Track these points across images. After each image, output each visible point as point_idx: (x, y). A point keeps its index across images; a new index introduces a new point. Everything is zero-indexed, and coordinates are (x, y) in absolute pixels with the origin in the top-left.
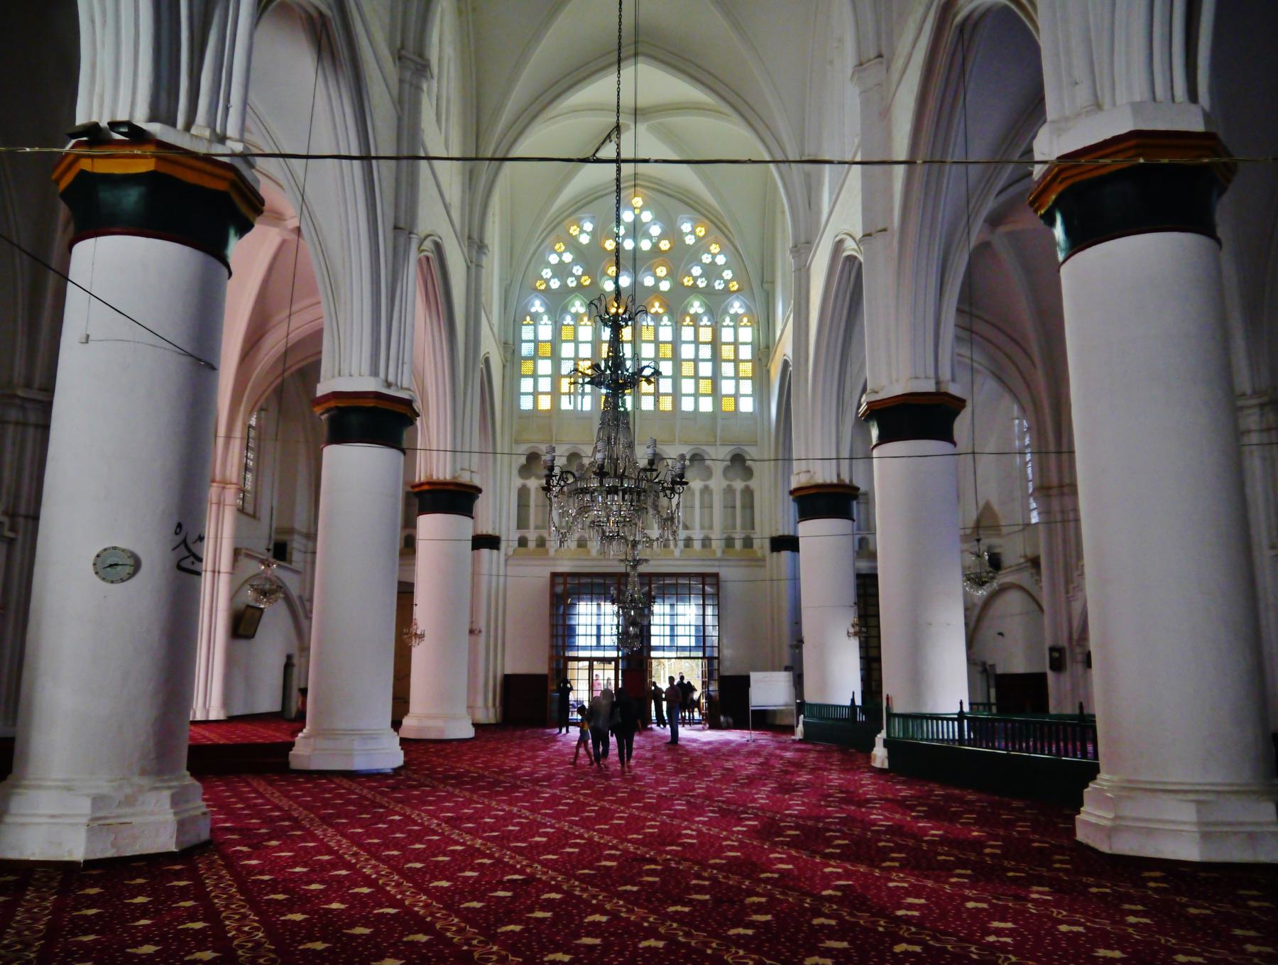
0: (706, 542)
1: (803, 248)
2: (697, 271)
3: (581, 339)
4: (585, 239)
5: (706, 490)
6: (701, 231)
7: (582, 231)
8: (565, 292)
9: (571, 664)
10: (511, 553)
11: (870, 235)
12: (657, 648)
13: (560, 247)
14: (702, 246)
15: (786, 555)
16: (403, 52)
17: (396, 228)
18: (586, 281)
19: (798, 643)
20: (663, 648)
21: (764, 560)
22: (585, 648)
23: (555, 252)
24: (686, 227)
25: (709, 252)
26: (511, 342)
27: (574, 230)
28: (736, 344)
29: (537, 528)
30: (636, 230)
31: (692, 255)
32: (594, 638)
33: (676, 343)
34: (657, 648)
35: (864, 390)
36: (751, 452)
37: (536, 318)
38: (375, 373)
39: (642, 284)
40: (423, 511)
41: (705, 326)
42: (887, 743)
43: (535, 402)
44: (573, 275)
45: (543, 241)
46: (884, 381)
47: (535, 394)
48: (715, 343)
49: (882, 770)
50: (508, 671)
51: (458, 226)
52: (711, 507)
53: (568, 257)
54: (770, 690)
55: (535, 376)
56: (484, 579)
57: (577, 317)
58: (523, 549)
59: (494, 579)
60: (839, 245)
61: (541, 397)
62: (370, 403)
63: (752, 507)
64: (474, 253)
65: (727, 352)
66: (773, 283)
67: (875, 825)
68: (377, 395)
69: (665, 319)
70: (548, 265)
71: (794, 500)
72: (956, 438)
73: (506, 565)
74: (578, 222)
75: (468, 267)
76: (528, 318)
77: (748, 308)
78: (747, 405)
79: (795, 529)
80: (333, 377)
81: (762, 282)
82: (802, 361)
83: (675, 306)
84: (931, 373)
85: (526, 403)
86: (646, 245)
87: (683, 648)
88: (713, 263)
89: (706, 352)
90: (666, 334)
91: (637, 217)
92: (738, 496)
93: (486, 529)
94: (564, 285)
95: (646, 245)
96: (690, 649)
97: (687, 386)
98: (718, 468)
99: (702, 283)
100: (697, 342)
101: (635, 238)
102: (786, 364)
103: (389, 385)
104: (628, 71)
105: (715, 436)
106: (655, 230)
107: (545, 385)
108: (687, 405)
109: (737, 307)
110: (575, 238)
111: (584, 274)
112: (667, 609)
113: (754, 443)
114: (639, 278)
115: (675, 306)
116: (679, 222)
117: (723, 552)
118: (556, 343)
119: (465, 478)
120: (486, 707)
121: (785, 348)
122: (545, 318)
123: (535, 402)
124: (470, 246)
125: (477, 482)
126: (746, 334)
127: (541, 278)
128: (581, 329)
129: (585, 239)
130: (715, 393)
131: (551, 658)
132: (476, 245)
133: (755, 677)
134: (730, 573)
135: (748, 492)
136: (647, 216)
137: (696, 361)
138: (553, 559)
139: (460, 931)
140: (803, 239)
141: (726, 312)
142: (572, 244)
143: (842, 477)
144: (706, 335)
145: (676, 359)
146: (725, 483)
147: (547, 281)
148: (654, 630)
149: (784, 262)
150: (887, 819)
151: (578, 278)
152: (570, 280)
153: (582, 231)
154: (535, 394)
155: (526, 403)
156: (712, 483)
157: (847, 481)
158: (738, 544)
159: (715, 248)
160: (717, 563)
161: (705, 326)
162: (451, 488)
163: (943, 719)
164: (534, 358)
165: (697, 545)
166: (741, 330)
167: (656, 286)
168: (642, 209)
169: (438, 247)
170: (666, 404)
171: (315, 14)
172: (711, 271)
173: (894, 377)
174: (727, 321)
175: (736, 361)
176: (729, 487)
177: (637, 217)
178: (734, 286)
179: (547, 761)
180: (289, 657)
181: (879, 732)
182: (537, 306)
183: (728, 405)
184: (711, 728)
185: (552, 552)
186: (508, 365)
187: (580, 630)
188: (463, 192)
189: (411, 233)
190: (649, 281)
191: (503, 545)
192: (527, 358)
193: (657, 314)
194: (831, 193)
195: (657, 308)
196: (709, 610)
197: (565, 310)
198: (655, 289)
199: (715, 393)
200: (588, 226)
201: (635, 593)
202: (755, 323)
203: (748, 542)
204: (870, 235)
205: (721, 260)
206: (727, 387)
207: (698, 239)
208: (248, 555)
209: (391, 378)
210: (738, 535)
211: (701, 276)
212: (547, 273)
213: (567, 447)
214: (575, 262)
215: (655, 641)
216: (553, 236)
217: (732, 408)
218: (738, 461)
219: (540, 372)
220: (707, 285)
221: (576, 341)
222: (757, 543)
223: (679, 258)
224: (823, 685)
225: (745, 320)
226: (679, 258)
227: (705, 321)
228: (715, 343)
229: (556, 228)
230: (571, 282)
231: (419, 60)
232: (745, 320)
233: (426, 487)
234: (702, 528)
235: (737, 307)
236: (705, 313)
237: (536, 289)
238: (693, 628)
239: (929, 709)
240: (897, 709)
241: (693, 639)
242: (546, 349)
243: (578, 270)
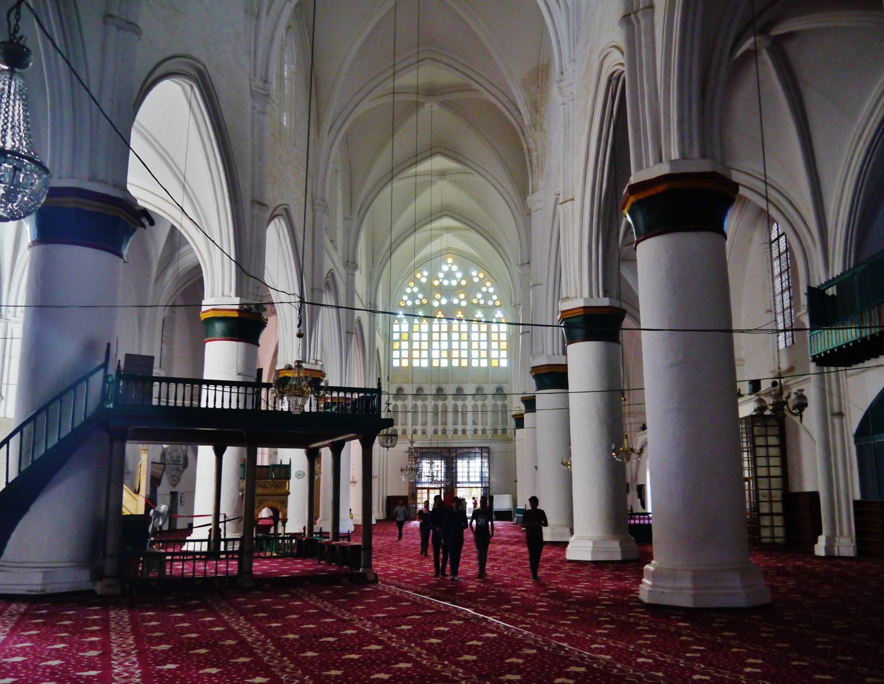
0: (484, 431)
2: (479, 296)
4: (424, 280)
6: (481, 275)
7: (422, 276)
8: (414, 307)
9: (419, 491)
12: (459, 483)
14: (482, 282)
18: (425, 301)
20: (463, 482)
22: (425, 483)
24: (474, 273)
27: (418, 276)
29: (402, 425)
30: (449, 275)
31: (477, 287)
33: (469, 333)
34: (459, 483)
39: (452, 303)
47: (400, 359)
53: (416, 290)
55: (400, 350)
61: (403, 360)
70: (406, 293)
78: (504, 363)
85: (396, 363)
87: (472, 482)
88: (487, 292)
94: (414, 304)
96: (475, 482)
97: (475, 354)
99: (482, 302)
107: (405, 354)
108: (475, 363)
109: (499, 314)
110: (419, 280)
120: (379, 512)
128: (422, 326)
129: (424, 280)
130: (489, 358)
131: (409, 488)
134: (495, 447)
136: (455, 268)
139: (364, 625)
142: (417, 282)
145: (469, 341)
146: (493, 402)
147: (405, 302)
148: (459, 474)
151: (421, 300)
153: (422, 276)
154: (400, 359)
158: (499, 432)
159: (488, 284)
164: (400, 340)
165: (480, 432)
167: (459, 303)
168: (452, 264)
172: (487, 296)
175: (499, 341)
178: (498, 303)
183: (495, 363)
190: (456, 301)
192: (396, 341)
196: (486, 464)
198: (458, 306)
199: (489, 358)
200: (426, 273)
201: (450, 456)
205: (491, 290)
206: (494, 354)
207: (481, 280)
210: (500, 427)
212: (405, 298)
214: (419, 292)
215: (459, 480)
216: (408, 280)
219: (402, 348)
226: (470, 289)
229: (410, 275)
230: (418, 302)
234: (482, 424)
235: (499, 314)
237: (400, 306)
242: (405, 336)
243: (420, 296)
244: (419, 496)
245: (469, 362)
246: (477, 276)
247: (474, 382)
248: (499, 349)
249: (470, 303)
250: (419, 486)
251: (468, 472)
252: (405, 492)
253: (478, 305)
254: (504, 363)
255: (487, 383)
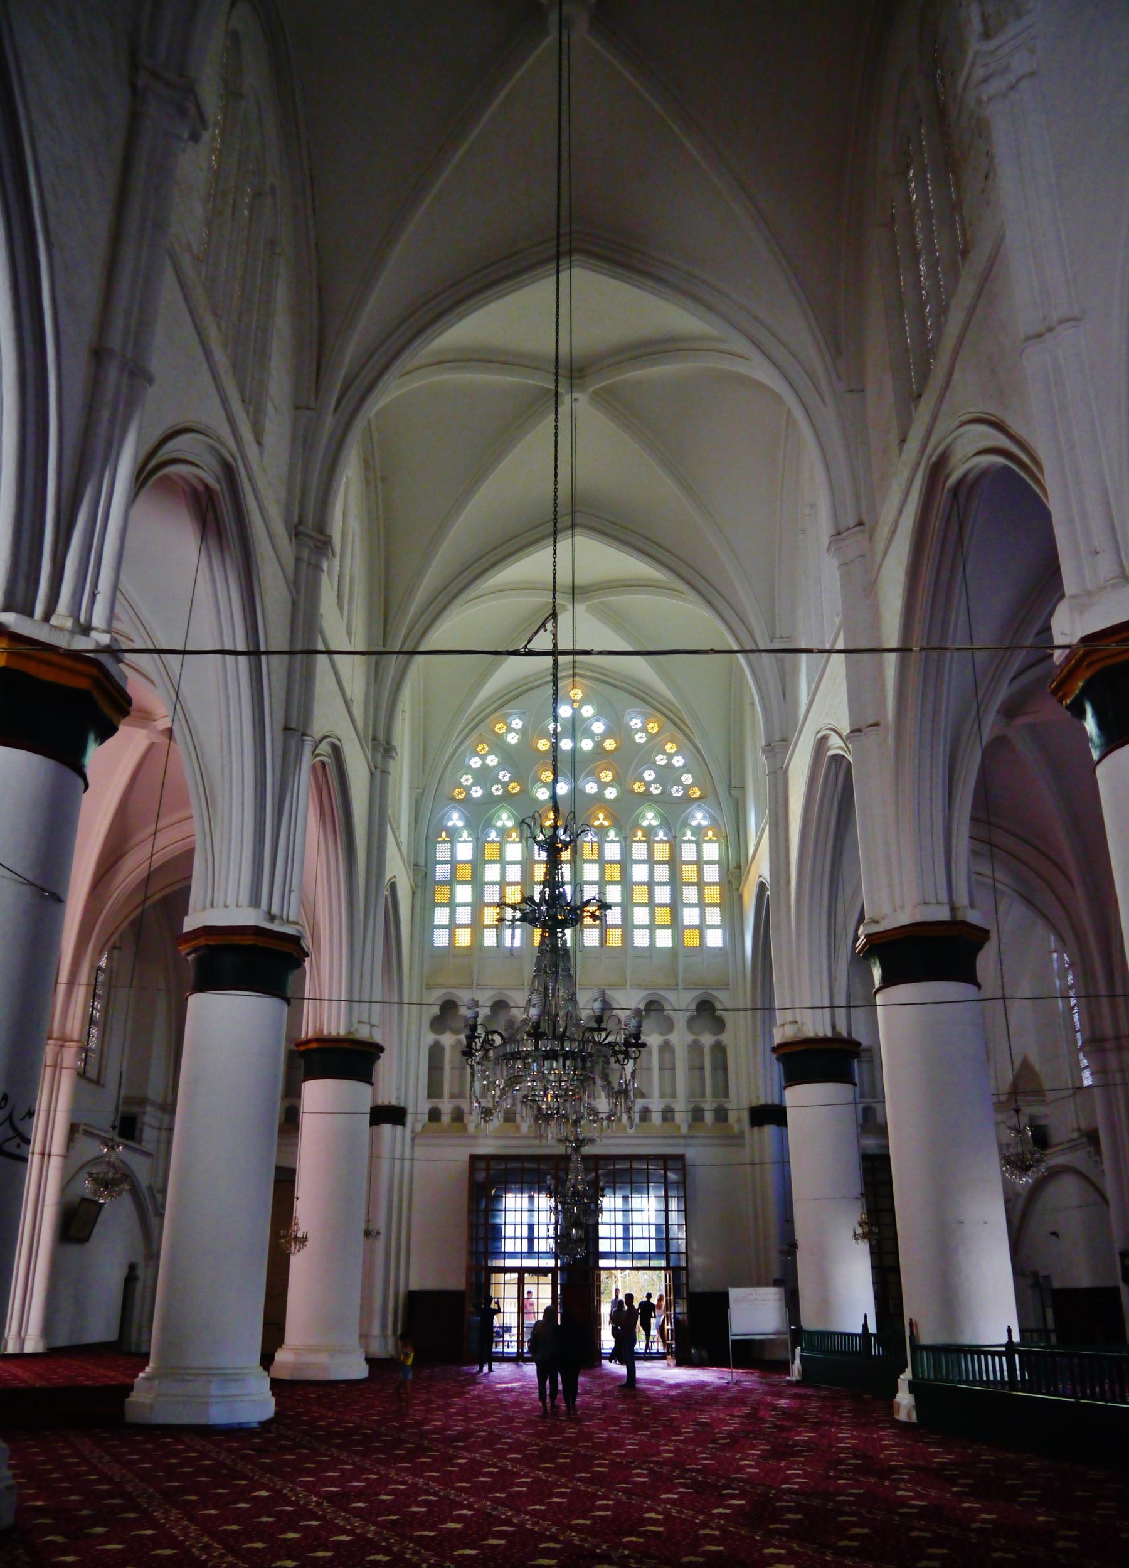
0: (668, 1114)
1: (778, 747)
2: (649, 775)
3: (509, 858)
4: (513, 739)
5: (666, 1047)
6: (653, 728)
7: (510, 730)
8: (490, 801)
9: (498, 1278)
10: (419, 1128)
11: (859, 730)
13: (483, 748)
14: (655, 744)
15: (769, 1130)
16: (301, 528)
17: (286, 729)
18: (515, 788)
19: (790, 1247)
20: (613, 1255)
21: (741, 1136)
22: (513, 1255)
23: (477, 754)
24: (636, 723)
25: (664, 752)
26: (422, 863)
27: (500, 728)
28: (699, 863)
29: (452, 1096)
30: (576, 727)
31: (643, 756)
32: (525, 1242)
33: (625, 863)
35: (861, 920)
36: (723, 998)
37: (453, 836)
38: (255, 902)
39: (583, 792)
40: (311, 1076)
41: (662, 841)
42: (913, 1387)
43: (452, 937)
44: (498, 782)
45: (461, 742)
46: (886, 909)
47: (452, 927)
48: (674, 863)
49: (907, 1425)
50: (414, 1286)
51: (360, 724)
52: (673, 1069)
53: (492, 761)
54: (755, 1313)
55: (451, 905)
56: (385, 1165)
57: (504, 832)
58: (435, 1125)
59: (397, 1163)
60: (821, 744)
61: (459, 931)
62: (248, 941)
63: (725, 1069)
64: (379, 756)
65: (689, 873)
66: (743, 788)
67: (904, 1506)
68: (257, 930)
69: (612, 834)
70: (469, 770)
71: (778, 1059)
72: (980, 980)
73: (413, 1146)
74: (505, 719)
75: (372, 774)
76: (444, 834)
77: (713, 819)
78: (715, 939)
79: (781, 1096)
80: (204, 908)
81: (730, 787)
82: (783, 881)
83: (623, 817)
84: (943, 896)
85: (441, 939)
86: (587, 745)
87: (641, 1255)
88: (669, 766)
89: (662, 873)
90: (613, 851)
91: (576, 713)
92: (707, 1051)
93: (388, 1096)
94: (488, 795)
95: (587, 745)
96: (650, 1255)
97: (641, 915)
98: (680, 1020)
99: (656, 790)
100: (651, 861)
101: (574, 738)
102: (762, 887)
103: (272, 918)
104: (564, 545)
105: (676, 978)
106: (598, 728)
107: (464, 916)
108: (641, 939)
109: (699, 818)
110: (500, 737)
111: (512, 780)
112: (619, 1202)
113: (725, 986)
114: (579, 785)
115: (623, 817)
116: (626, 718)
117: (690, 1127)
118: (478, 863)
119: (363, 1033)
121: (761, 868)
122: (465, 834)
123: (452, 937)
124: (374, 749)
125: (378, 1039)
126: (712, 851)
127: (460, 785)
129: (513, 739)
130: (675, 923)
131: (469, 1269)
132: (381, 747)
133: (734, 1293)
135: (720, 1050)
137: (650, 884)
138: (474, 1137)
140: (777, 737)
141: (686, 824)
142: (498, 745)
143: (838, 1029)
144: (662, 851)
145: (626, 882)
146: (690, 1038)
147: (467, 789)
148: (603, 1231)
149: (756, 764)
150: (919, 1497)
151: (505, 785)
152: (495, 787)
153: (510, 730)
154: (452, 927)
155: (441, 939)
156: (674, 1038)
157: (845, 1034)
158: (709, 1117)
159: (670, 748)
160: (682, 1141)
161: (662, 841)
162: (346, 1045)
163: (986, 1353)
164: (452, 882)
165: (656, 1118)
166: (705, 846)
169: (336, 751)
170: (615, 938)
171: (201, 488)
172: (667, 775)
173: (898, 903)
174: (688, 835)
175: (700, 884)
176: (695, 1042)
177: (576, 713)
178: (696, 793)
179: (463, 1411)
180: (132, 1268)
181: (903, 1371)
182: (455, 820)
183: (691, 939)
184: (679, 1364)
185: (471, 1128)
186: (419, 891)
187: (508, 1231)
188: (368, 685)
189: (304, 734)
190: (591, 788)
191: (409, 1119)
192: (441, 883)
193: (601, 826)
194: (809, 683)
195: (601, 820)
196: (674, 1204)
197: (489, 824)
198: (599, 798)
199: (675, 923)
200: (517, 724)
201: (579, 1184)
202: (722, 838)
203: (721, 1115)
204: (859, 730)
205: (678, 761)
206: (690, 916)
207: (651, 737)
208: (87, 1133)
209: (275, 910)
210: (709, 1105)
211: (654, 781)
212: (467, 779)
213: (493, 992)
214: (501, 766)
215: (604, 1246)
216: (475, 734)
217: (697, 943)
218: (706, 1011)
219: (458, 900)
220: (662, 793)
221: (503, 862)
222: (732, 1117)
223: (627, 759)
224: (825, 1305)
225: (710, 833)
227: (661, 835)
228: (674, 863)
231: (321, 537)
232: (710, 833)
233: (314, 1045)
234: (662, 1096)
235: (699, 818)
236: (660, 826)
237: (453, 799)
238: (653, 1228)
239: (967, 1339)
240: (925, 1339)
241: (653, 1242)
242: (466, 872)
243: (504, 776)
244: (496, 1291)
245: (627, 936)
246: (644, 729)
247: (640, 987)
248: (702, 905)
249: (626, 793)
250: (499, 1263)
251: (626, 1227)
252: (455, 1281)
253: (647, 796)
254: (715, 939)
255: (675, 988)
